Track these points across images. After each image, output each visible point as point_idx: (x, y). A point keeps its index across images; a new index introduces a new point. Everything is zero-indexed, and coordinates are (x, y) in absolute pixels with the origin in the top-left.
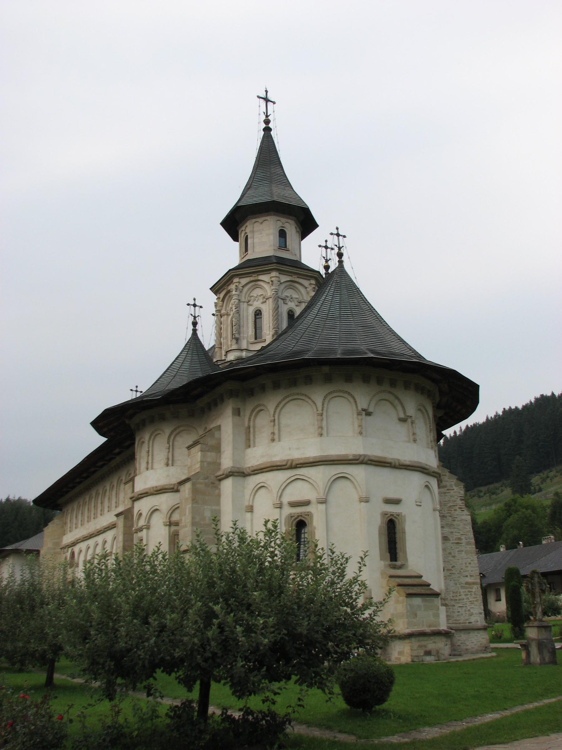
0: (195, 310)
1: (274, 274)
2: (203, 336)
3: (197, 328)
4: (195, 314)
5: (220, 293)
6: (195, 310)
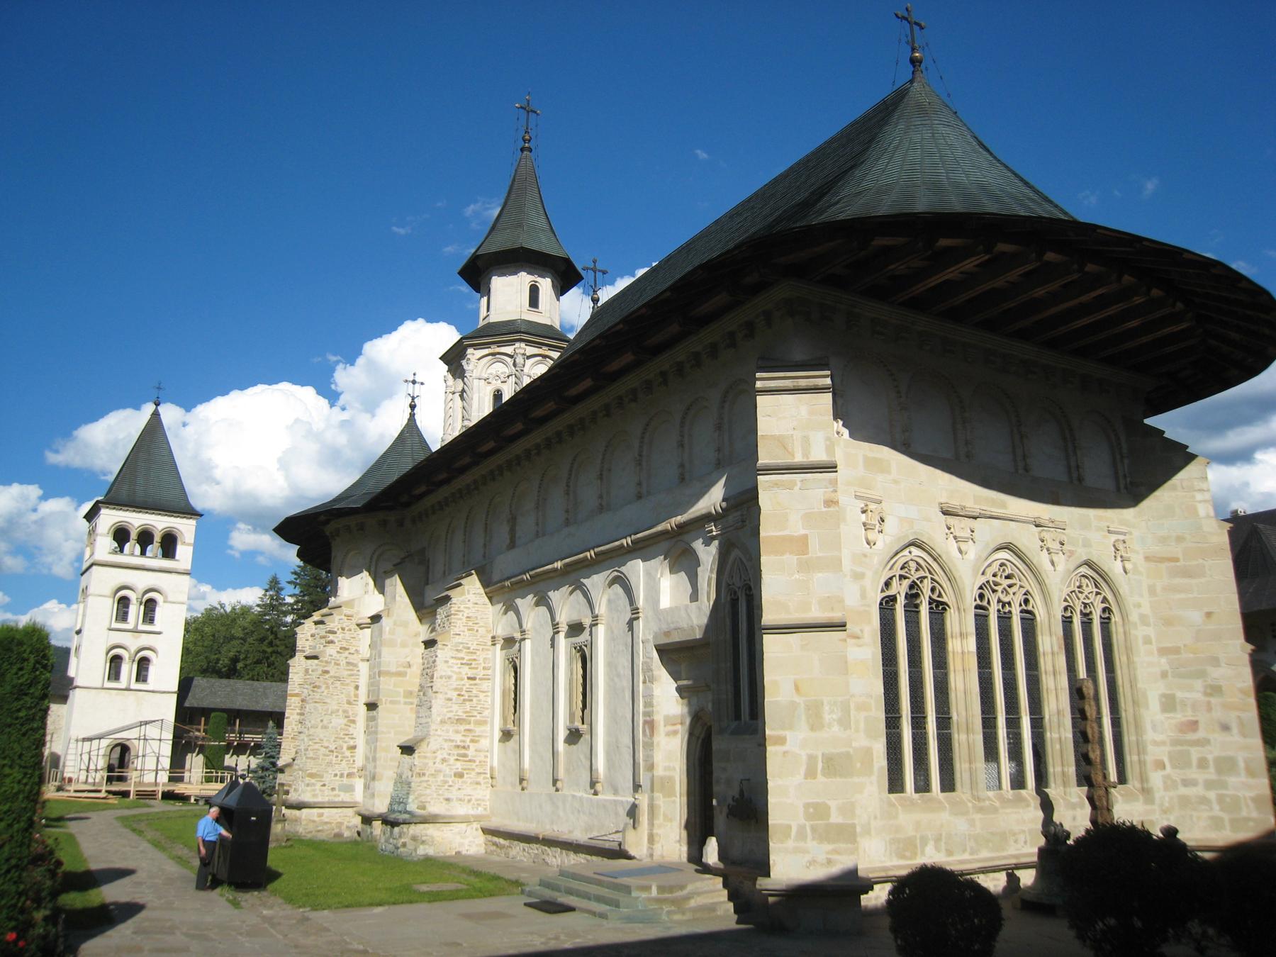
0: (414, 388)
1: (517, 345)
2: (421, 422)
3: (415, 411)
4: (413, 393)
5: (452, 365)
6: (414, 388)
